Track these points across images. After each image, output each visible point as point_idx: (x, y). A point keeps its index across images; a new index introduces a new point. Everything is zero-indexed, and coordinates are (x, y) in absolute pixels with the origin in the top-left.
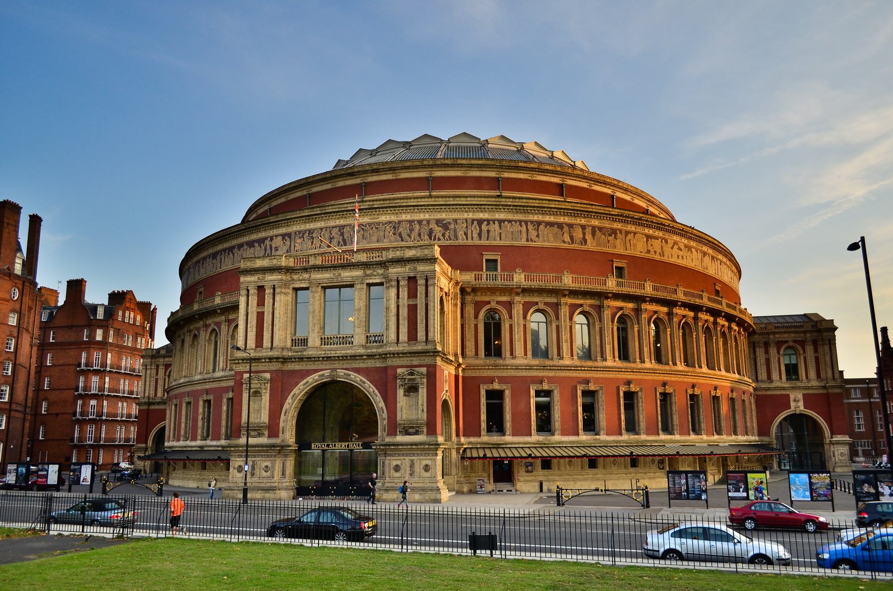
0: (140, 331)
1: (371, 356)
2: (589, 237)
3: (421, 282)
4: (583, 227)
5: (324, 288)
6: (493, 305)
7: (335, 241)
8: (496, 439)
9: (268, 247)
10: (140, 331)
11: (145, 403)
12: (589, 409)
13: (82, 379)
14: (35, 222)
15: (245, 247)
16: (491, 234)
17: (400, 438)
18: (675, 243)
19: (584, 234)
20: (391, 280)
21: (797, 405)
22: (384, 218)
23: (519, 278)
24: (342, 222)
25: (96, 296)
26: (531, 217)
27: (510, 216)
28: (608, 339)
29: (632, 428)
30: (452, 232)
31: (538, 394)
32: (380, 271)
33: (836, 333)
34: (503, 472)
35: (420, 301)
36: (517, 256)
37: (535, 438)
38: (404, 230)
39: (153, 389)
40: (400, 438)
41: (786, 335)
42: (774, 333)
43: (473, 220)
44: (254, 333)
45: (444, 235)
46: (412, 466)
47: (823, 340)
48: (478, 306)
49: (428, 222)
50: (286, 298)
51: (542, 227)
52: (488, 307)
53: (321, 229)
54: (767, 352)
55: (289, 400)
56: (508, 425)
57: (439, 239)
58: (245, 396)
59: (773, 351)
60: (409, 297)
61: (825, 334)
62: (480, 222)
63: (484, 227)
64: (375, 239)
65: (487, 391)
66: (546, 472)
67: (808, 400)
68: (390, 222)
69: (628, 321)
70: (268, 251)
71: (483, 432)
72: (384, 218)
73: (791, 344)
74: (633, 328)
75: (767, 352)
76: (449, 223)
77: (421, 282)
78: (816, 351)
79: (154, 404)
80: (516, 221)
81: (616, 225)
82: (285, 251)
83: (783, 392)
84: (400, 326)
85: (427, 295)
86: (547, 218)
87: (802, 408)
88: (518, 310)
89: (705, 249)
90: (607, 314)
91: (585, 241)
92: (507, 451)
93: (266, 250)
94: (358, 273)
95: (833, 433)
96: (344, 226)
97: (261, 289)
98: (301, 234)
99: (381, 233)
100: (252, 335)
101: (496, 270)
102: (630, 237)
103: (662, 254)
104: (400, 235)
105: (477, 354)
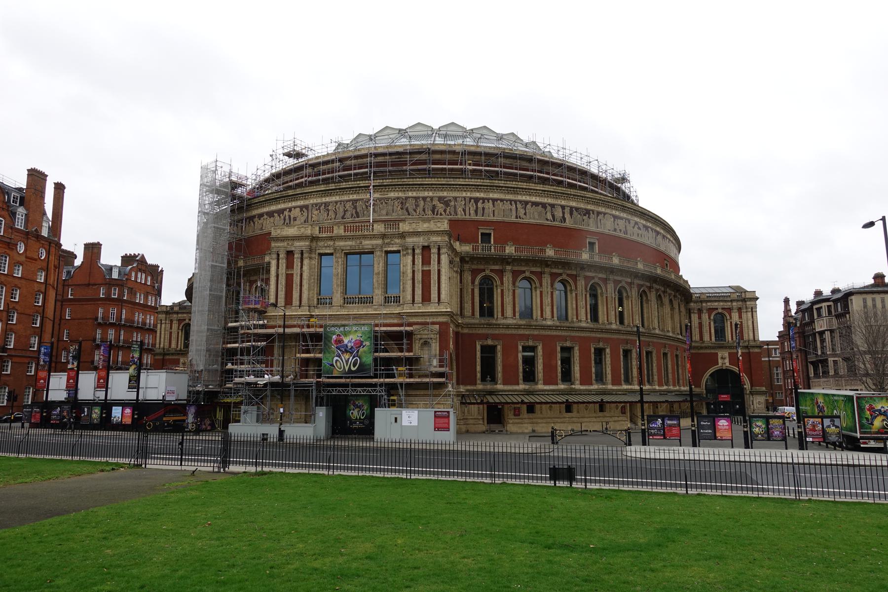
0: (149, 290)
2: (567, 216)
3: (434, 250)
4: (563, 207)
5: (347, 254)
6: (488, 272)
7: (348, 214)
8: (489, 387)
9: (287, 217)
10: (149, 290)
11: (160, 354)
12: (567, 362)
13: (99, 331)
14: (60, 188)
15: (265, 217)
16: (486, 211)
18: (636, 223)
19: (563, 213)
20: (407, 249)
21: (724, 361)
22: (392, 195)
23: (510, 250)
24: (355, 197)
25: (110, 258)
26: (520, 198)
27: (502, 196)
28: (582, 303)
29: (600, 378)
30: (452, 209)
31: (525, 349)
32: (397, 241)
33: (757, 302)
34: (496, 416)
35: (434, 267)
36: (509, 231)
37: (522, 387)
38: (410, 205)
39: (167, 341)
41: (716, 304)
42: (707, 301)
43: (471, 198)
44: (283, 293)
45: (445, 211)
47: (746, 308)
48: (475, 273)
49: (432, 198)
50: (313, 262)
51: (529, 206)
52: (483, 274)
53: (336, 202)
54: (700, 318)
56: (500, 375)
57: (441, 214)
59: (705, 316)
60: (423, 264)
61: (748, 303)
62: (477, 200)
63: (480, 205)
64: (384, 212)
65: (483, 348)
66: (531, 415)
67: (733, 359)
68: (398, 198)
69: (598, 289)
70: (287, 221)
71: (479, 382)
72: (392, 195)
73: (720, 311)
74: (602, 296)
75: (700, 318)
76: (450, 201)
79: (168, 354)
80: (507, 201)
81: (589, 207)
82: (303, 221)
83: (713, 351)
84: (416, 289)
85: (439, 262)
86: (534, 199)
87: (728, 364)
88: (508, 278)
89: (658, 229)
90: (581, 283)
91: (565, 219)
92: (500, 397)
93: (285, 219)
94: (379, 242)
95: (752, 386)
96: (356, 201)
97: (290, 254)
98: (318, 206)
99: (390, 208)
100: (282, 294)
101: (490, 242)
102: (601, 217)
103: (626, 233)
104: (407, 210)
105: (473, 314)
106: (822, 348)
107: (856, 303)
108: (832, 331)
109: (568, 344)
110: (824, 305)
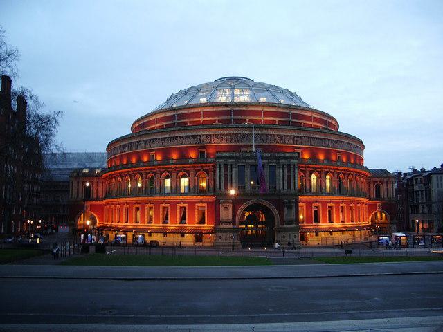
1: (273, 195)
3: (292, 166)
17: (285, 226)
20: (280, 165)
22: (257, 132)
24: (237, 132)
40: (285, 226)
46: (290, 235)
55: (239, 211)
58: (222, 209)
59: (372, 185)
62: (294, 136)
70: (199, 141)
77: (292, 166)
78: (387, 186)
91: (329, 146)
97: (226, 166)
98: (217, 136)
106: (417, 199)
107: (434, 178)
108: (422, 191)
109: (331, 204)
110: (419, 178)
